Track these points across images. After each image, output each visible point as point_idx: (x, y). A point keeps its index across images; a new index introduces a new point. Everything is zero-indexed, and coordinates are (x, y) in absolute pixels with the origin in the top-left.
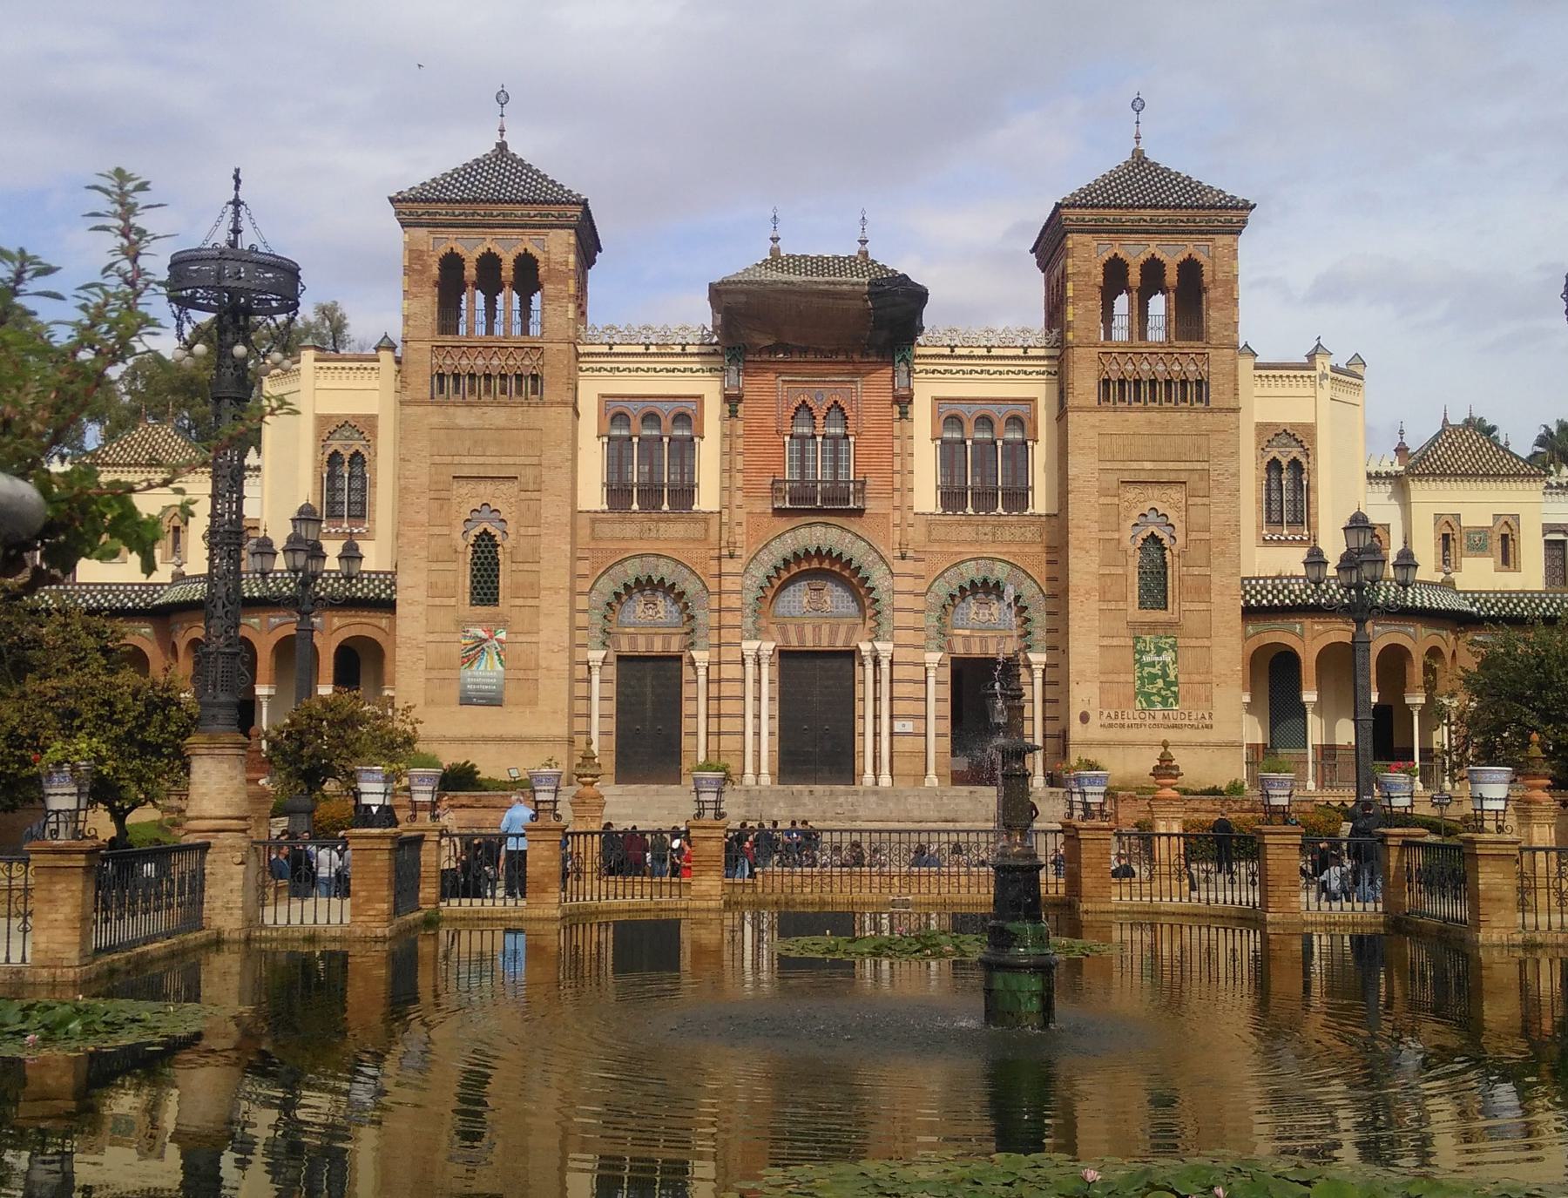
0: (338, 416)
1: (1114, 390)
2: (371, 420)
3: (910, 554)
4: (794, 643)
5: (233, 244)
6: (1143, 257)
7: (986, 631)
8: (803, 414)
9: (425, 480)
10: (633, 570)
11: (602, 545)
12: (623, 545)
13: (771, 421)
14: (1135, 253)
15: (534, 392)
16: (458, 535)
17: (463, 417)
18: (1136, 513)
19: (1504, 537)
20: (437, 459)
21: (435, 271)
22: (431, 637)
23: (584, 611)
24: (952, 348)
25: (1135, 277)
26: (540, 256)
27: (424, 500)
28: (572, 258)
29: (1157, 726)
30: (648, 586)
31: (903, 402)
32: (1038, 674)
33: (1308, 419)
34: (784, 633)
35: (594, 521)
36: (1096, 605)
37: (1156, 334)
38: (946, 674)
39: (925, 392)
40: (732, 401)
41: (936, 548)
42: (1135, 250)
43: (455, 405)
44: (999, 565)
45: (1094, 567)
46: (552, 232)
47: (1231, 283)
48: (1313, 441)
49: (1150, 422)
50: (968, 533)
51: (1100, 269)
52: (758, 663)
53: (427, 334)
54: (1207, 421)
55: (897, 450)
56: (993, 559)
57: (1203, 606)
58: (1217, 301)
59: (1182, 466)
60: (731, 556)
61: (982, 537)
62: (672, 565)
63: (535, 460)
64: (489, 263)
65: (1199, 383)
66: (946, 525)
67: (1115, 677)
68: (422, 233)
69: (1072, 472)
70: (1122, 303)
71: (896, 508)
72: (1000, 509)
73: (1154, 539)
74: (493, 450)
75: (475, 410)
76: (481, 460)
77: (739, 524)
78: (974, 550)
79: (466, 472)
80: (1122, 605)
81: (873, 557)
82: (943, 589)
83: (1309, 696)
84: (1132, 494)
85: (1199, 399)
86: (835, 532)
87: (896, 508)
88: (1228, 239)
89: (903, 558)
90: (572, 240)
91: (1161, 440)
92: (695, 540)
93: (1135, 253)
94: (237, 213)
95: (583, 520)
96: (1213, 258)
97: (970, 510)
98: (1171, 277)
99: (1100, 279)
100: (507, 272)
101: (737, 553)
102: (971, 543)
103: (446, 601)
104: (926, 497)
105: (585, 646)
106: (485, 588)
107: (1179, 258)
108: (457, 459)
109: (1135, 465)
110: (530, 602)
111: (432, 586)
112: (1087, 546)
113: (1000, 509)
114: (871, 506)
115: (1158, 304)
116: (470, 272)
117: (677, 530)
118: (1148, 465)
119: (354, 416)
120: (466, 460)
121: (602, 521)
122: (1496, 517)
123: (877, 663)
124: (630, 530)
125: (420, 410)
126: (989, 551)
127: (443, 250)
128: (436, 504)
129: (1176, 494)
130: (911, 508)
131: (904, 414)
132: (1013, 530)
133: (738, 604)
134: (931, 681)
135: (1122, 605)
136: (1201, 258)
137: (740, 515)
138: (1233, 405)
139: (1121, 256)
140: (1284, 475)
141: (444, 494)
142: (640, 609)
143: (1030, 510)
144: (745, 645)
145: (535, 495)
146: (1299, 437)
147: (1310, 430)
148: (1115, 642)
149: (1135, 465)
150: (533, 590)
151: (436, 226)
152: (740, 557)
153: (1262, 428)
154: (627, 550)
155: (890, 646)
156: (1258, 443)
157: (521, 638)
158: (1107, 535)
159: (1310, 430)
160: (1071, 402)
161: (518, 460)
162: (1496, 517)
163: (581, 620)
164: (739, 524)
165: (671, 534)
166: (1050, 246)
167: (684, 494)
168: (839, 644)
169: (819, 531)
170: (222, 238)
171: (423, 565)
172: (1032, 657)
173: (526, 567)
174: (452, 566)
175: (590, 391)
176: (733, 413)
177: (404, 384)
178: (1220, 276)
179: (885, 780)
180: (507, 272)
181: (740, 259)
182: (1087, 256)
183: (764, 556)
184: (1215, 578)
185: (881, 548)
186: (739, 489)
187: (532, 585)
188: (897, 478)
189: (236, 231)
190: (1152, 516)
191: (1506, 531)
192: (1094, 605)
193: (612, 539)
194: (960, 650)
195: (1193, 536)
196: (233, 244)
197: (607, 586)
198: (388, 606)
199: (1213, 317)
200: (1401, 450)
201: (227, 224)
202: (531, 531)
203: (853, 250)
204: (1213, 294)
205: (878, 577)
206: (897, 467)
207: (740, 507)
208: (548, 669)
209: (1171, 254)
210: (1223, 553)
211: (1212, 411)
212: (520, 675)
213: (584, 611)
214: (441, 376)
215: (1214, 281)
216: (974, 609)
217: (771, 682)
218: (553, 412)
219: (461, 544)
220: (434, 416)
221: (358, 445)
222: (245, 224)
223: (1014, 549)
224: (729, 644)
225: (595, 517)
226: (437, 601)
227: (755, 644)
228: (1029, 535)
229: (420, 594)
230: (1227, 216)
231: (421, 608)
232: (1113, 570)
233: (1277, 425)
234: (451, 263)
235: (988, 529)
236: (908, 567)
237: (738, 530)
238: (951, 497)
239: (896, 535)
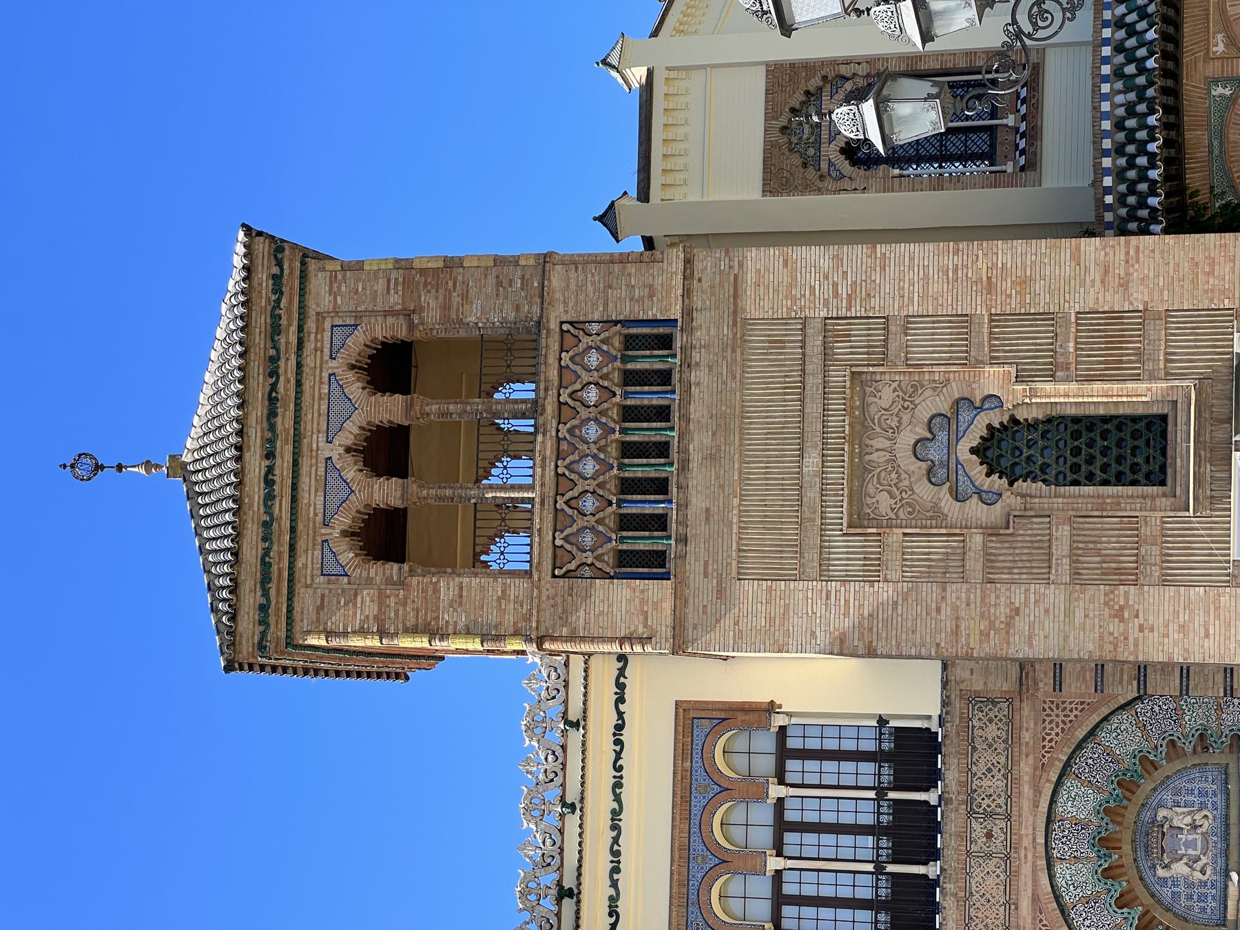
1: (643, 543)
14: (341, 489)
18: (925, 491)
24: (564, 893)
33: (758, 82)
36: (1152, 593)
44: (1066, 807)
45: (1055, 596)
49: (713, 458)
50: (986, 879)
56: (1049, 821)
58: (446, 307)
59: (814, 382)
61: (998, 844)
72: (931, 797)
78: (1029, 864)
85: (665, 342)
88: (319, 283)
96: (358, 316)
102: (1011, 875)
107: (355, 388)
109: (812, 494)
112: (1002, 611)
113: (931, 797)
118: (812, 461)
126: (1030, 825)
132: (980, 769)
139: (343, 521)
143: (934, 727)
149: (812, 494)
153: (776, 180)
156: (806, 188)
158: (975, 565)
178: (395, 300)
210: (1023, 283)
211: (688, 313)
215: (408, 314)
216: (1180, 868)
223: (1026, 768)
228: (992, 731)
232: (1061, 549)
235: (978, 829)
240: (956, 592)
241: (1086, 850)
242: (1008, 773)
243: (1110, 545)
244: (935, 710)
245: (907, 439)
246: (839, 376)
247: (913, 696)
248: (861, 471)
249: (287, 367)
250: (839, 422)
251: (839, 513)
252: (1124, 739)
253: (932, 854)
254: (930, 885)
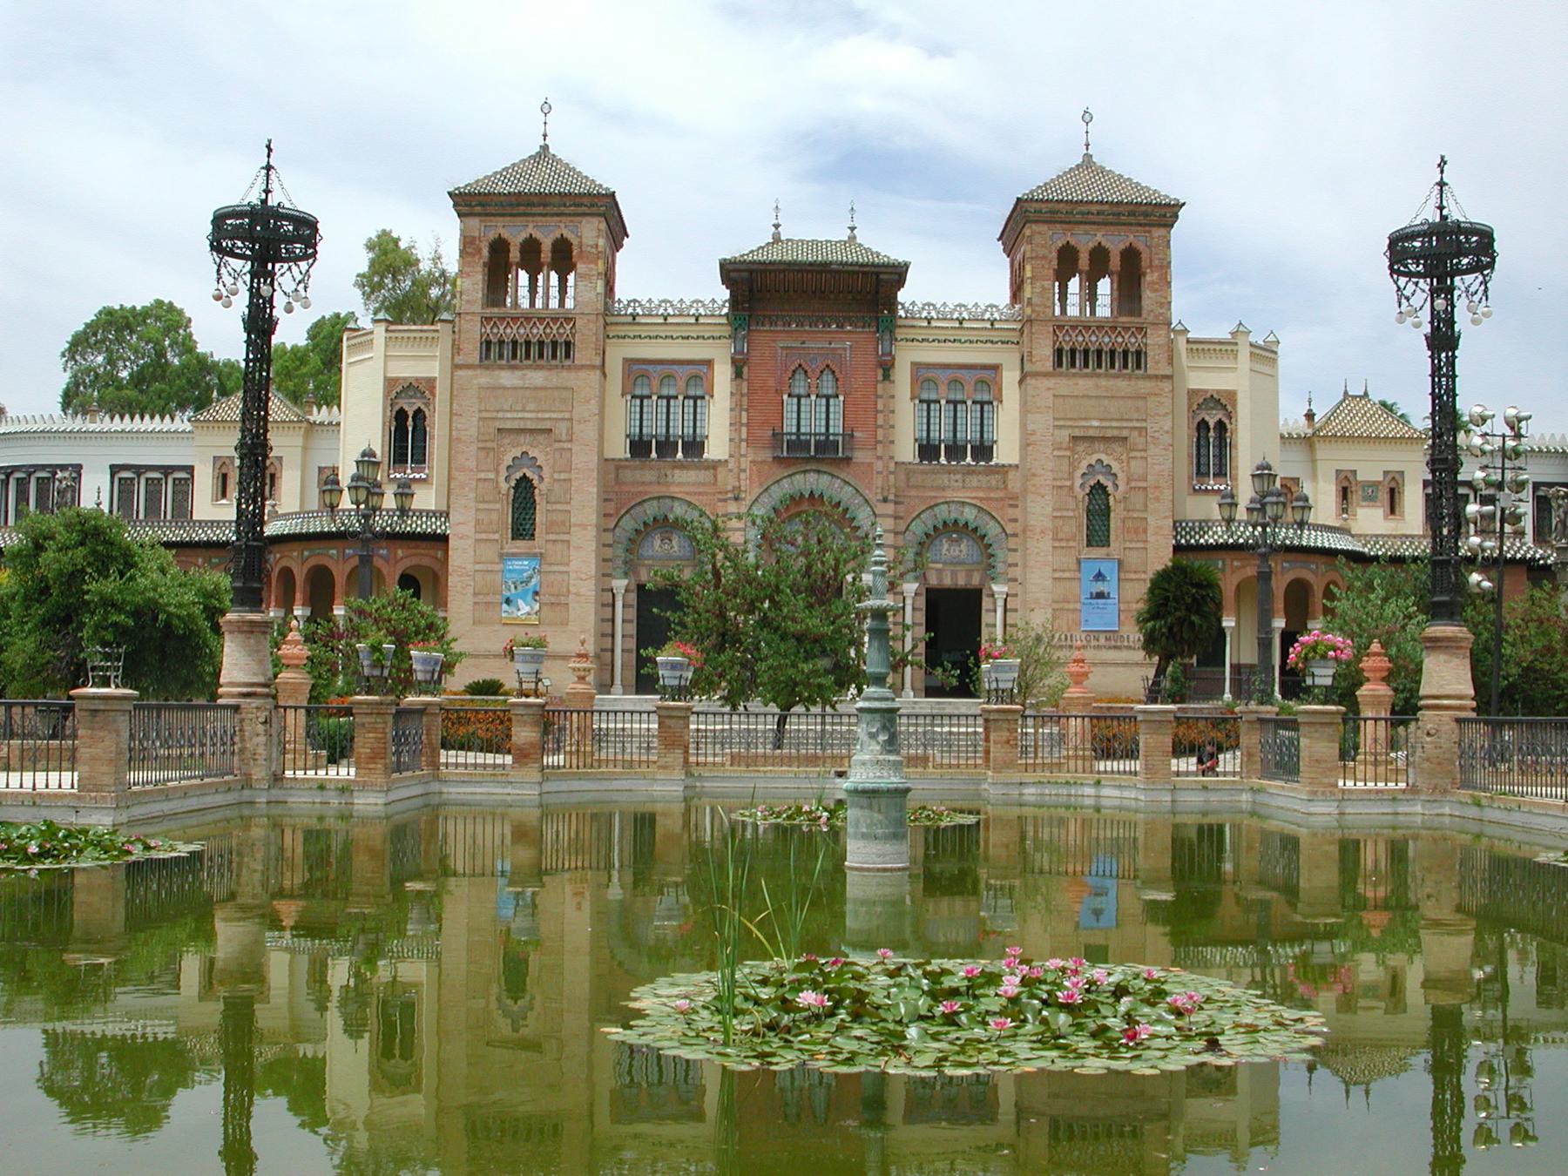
0: (405, 379)
2: (431, 382)
3: (891, 497)
5: (264, 202)
6: (1091, 245)
7: (951, 566)
8: (800, 376)
9: (474, 431)
10: (651, 510)
11: (625, 489)
12: (641, 489)
13: (771, 383)
14: (1085, 241)
15: (568, 356)
16: (502, 479)
17: (507, 378)
18: (1084, 464)
19: (1392, 491)
20: (484, 415)
21: (485, 252)
22: (478, 567)
23: (609, 546)
25: (1084, 262)
26: (575, 242)
27: (473, 448)
28: (601, 242)
29: (1099, 647)
30: (664, 525)
31: (887, 368)
32: (1000, 603)
35: (618, 468)
36: (1050, 543)
37: (1104, 310)
38: (922, 602)
39: (906, 357)
40: (739, 367)
41: (913, 493)
42: (1084, 239)
43: (501, 368)
44: (967, 510)
46: (584, 220)
47: (1166, 266)
48: (1234, 406)
51: (1055, 255)
53: (477, 308)
54: (1145, 386)
55: (880, 407)
57: (1140, 545)
60: (736, 499)
62: (685, 507)
63: (567, 415)
64: (531, 249)
65: (1138, 353)
66: (924, 472)
67: (1066, 606)
68: (474, 222)
69: (1030, 427)
70: (1074, 285)
71: (879, 458)
73: (1099, 489)
74: (531, 406)
75: (518, 373)
76: (520, 415)
79: (508, 425)
80: (1072, 544)
81: (858, 500)
82: (918, 528)
83: (1228, 623)
84: (1081, 448)
86: (825, 480)
87: (879, 458)
88: (1162, 231)
89: (885, 500)
90: (603, 226)
91: (1106, 402)
92: (704, 484)
93: (1085, 241)
94: (268, 175)
95: (611, 467)
97: (943, 460)
98: (1115, 262)
99: (1055, 262)
100: (546, 256)
103: (492, 536)
104: (906, 451)
105: (609, 575)
106: (522, 527)
107: (1122, 247)
108: (500, 415)
109: (1083, 423)
110: (565, 537)
111: (478, 522)
113: (969, 459)
114: (860, 456)
115: (1104, 286)
116: (515, 255)
117: (690, 476)
119: (417, 379)
120: (508, 415)
121: (626, 467)
122: (1386, 473)
124: (649, 476)
125: (470, 373)
127: (492, 235)
128: (482, 454)
129: (1117, 448)
130: (892, 458)
131: (886, 377)
134: (909, 609)
135: (1072, 544)
136: (1141, 246)
137: (745, 463)
138: (1168, 371)
139: (1072, 243)
140: (1212, 433)
141: (488, 445)
142: (657, 543)
145: (566, 445)
146: (1222, 402)
147: (1232, 395)
148: (1067, 575)
149: (1083, 423)
150: (564, 526)
151: (487, 215)
153: (1192, 393)
154: (646, 493)
156: (1190, 406)
157: (555, 568)
159: (1232, 395)
160: (1027, 367)
161: (554, 416)
162: (1386, 473)
163: (609, 552)
165: (683, 480)
166: (1011, 236)
167: (695, 446)
169: (812, 477)
170: (254, 198)
171: (472, 504)
172: (995, 588)
173: (558, 507)
174: (498, 506)
175: (618, 354)
176: (738, 374)
177: (456, 349)
178: (1156, 262)
180: (546, 256)
181: (747, 243)
182: (1045, 241)
184: (1151, 520)
185: (866, 493)
187: (563, 523)
188: (880, 432)
189: (267, 191)
190: (1098, 467)
191: (1393, 485)
192: (1047, 544)
193: (633, 484)
194: (933, 581)
195: (1133, 484)
196: (264, 202)
197: (628, 524)
198: (444, 539)
199: (1148, 297)
200: (1310, 416)
201: (260, 185)
202: (563, 476)
203: (844, 235)
204: (1150, 277)
205: (863, 516)
206: (880, 421)
208: (578, 595)
209: (1115, 243)
210: (1157, 499)
211: (1150, 377)
212: (553, 600)
213: (609, 546)
214: (489, 343)
215: (1151, 266)
218: (583, 374)
219: (504, 486)
220: (483, 378)
221: (419, 404)
222: (274, 185)
223: (981, 494)
225: (618, 465)
226: (484, 536)
228: (994, 483)
229: (469, 529)
230: (1163, 214)
231: (470, 542)
233: (1206, 391)
234: (499, 248)
235: (959, 477)
236: (889, 508)
237: (743, 476)
238: (927, 451)
239: (879, 481)
240: (1050, 475)
241: (953, 516)
242: (979, 488)
243: (1066, 529)
244: (1002, 461)
245: (1103, 457)
246: (1125, 433)
247: (1006, 452)
248: (1092, 439)
249: (1132, 219)
250: (1110, 433)
251: (1077, 433)
252: (992, 530)
253: (948, 459)
254: (938, 459)
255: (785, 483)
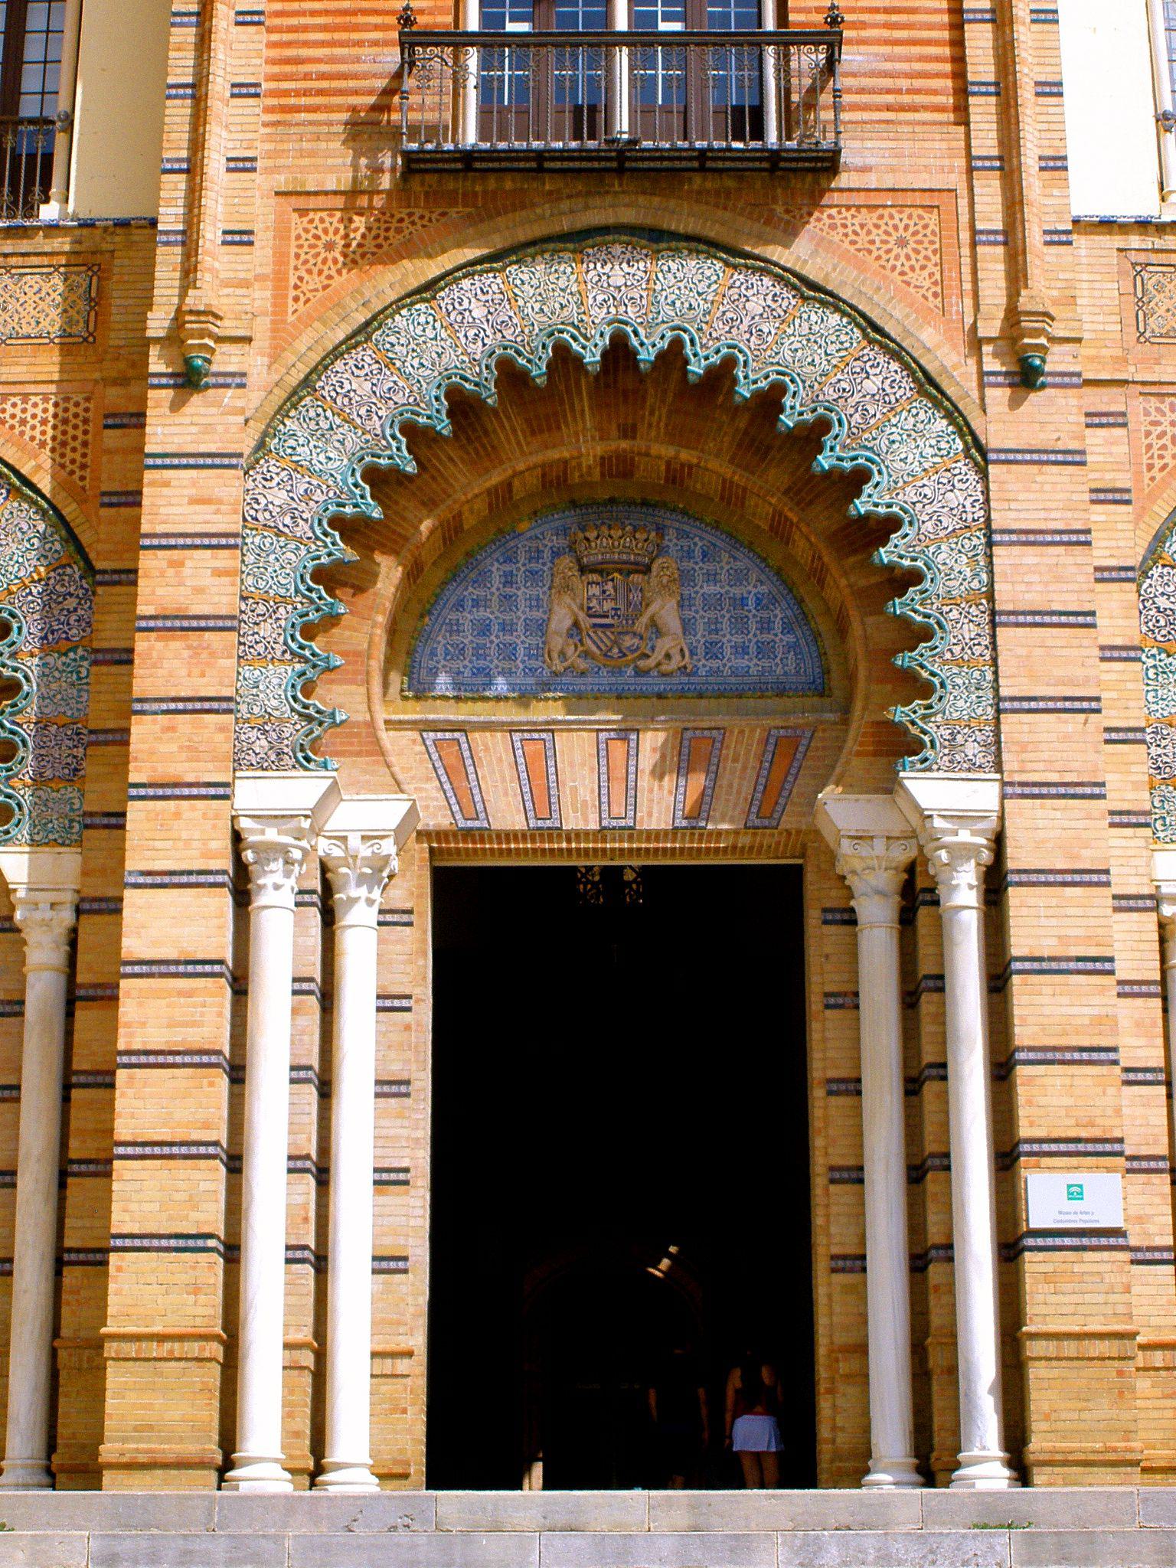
4: (507, 812)
34: (456, 773)
52: (326, 904)
77: (239, 238)
81: (883, 376)
101: (226, 360)
123: (917, 895)
133: (221, 599)
144: (254, 794)
152: (238, 380)
155: (983, 796)
164: (239, 238)
168: (727, 835)
179: (985, 1468)
183: (354, 380)
186: (243, 91)
207: (241, 165)
217: (389, 1003)
224: (168, 790)
227: (298, 790)
255: (473, 297)
